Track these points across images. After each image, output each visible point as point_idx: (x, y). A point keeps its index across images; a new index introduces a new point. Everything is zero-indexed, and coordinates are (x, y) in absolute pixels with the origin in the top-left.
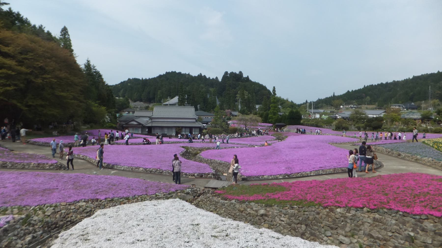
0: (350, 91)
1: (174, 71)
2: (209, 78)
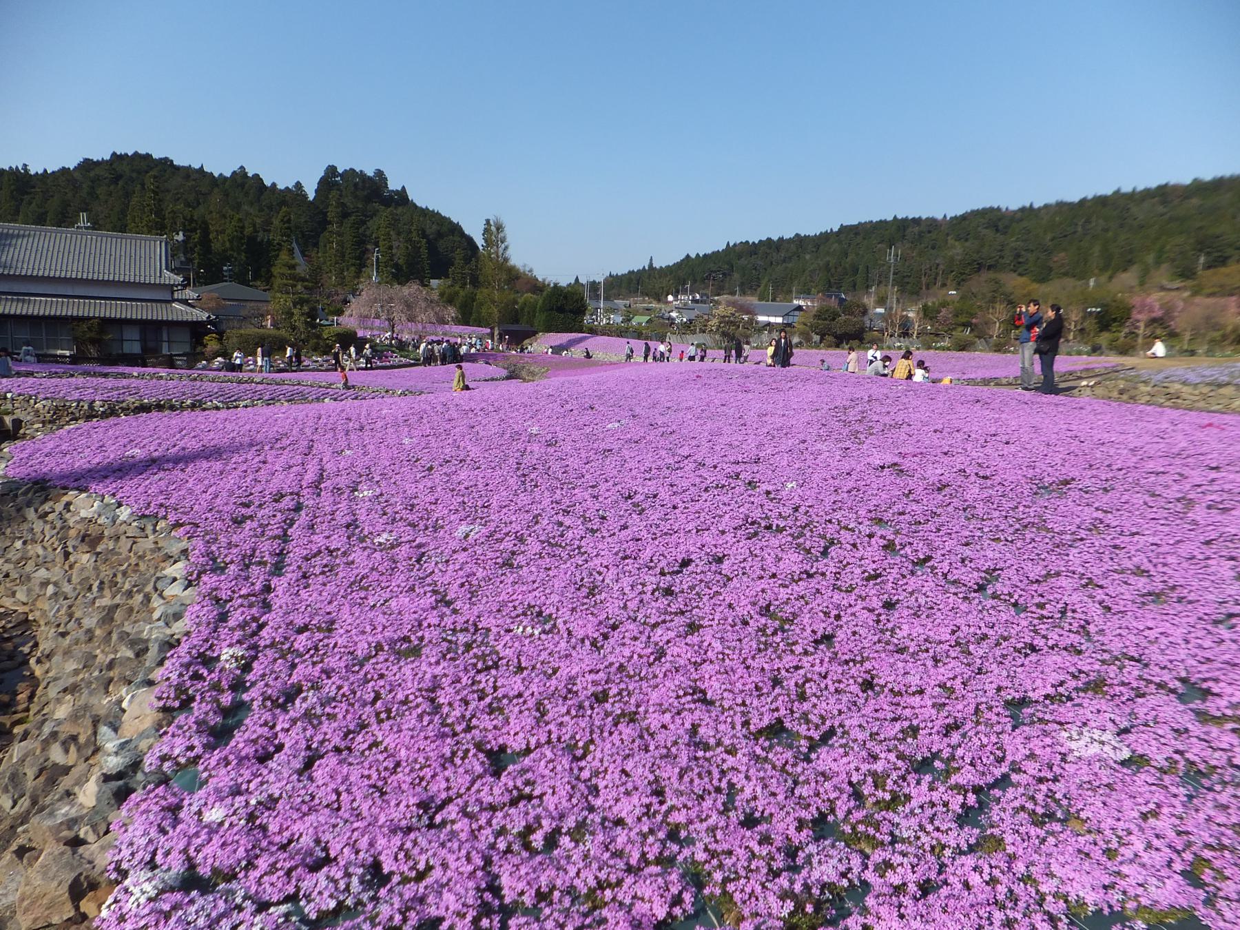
0: (693, 256)
1: (142, 151)
2: (274, 185)
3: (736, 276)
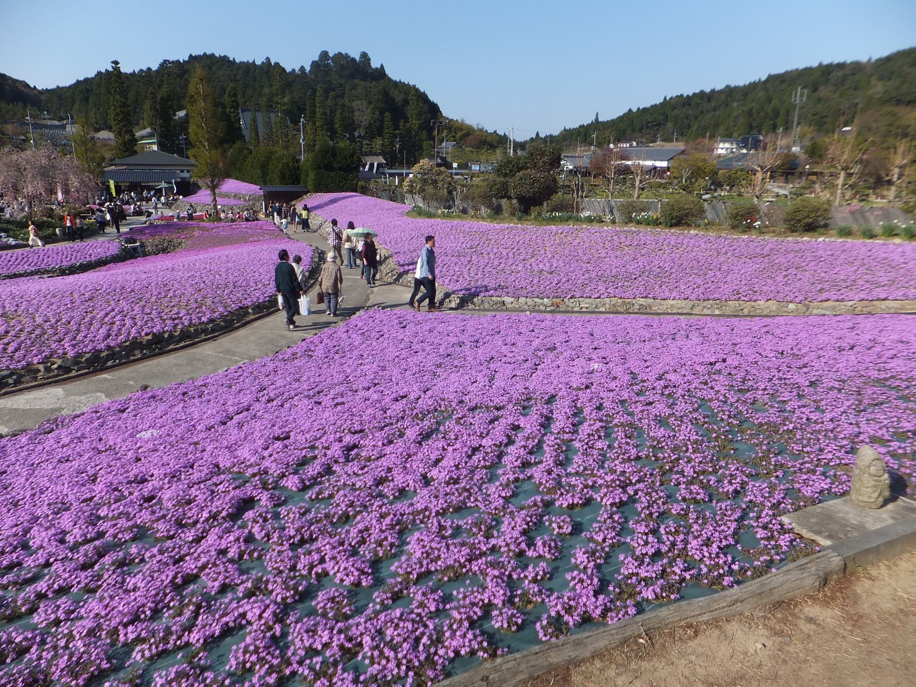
0: (635, 110)
3: (670, 125)
